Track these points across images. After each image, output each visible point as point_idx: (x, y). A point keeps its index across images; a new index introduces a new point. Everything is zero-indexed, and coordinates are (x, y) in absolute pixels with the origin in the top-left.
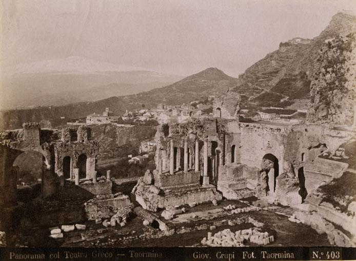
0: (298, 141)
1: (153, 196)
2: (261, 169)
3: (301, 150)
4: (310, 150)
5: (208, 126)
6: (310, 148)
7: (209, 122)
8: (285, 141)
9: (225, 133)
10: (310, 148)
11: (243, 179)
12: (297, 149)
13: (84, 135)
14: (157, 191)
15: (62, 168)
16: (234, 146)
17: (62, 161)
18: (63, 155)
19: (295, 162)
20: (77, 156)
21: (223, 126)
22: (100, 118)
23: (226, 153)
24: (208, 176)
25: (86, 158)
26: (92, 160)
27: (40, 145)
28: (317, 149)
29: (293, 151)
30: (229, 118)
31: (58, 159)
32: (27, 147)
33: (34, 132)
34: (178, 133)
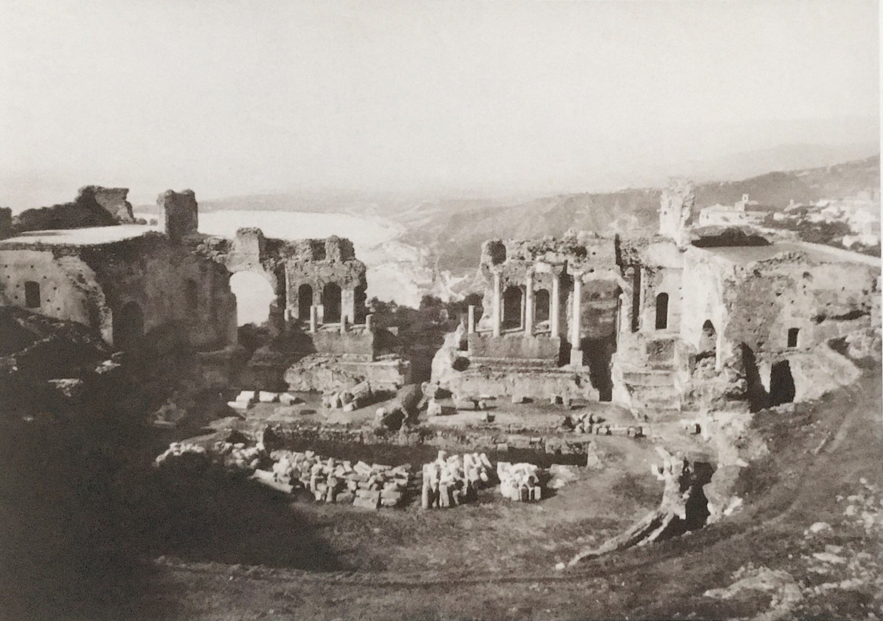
0: (778, 299)
2: (699, 352)
3: (787, 320)
4: (824, 324)
6: (820, 319)
7: (597, 241)
8: (733, 296)
9: (637, 266)
10: (820, 319)
11: (667, 368)
13: (334, 251)
15: (297, 302)
17: (297, 292)
19: (763, 347)
20: (322, 285)
21: (634, 251)
23: (641, 308)
25: (340, 290)
26: (348, 295)
28: (847, 323)
29: (759, 321)
31: (291, 287)
34: (522, 258)
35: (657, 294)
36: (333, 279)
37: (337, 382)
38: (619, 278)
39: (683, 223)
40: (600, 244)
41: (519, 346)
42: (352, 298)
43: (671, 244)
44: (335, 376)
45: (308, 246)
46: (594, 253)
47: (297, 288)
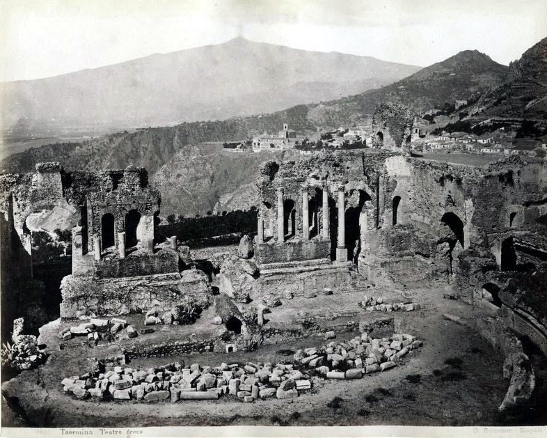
1: (245, 278)
5: (348, 164)
7: (349, 158)
12: (499, 207)
13: (134, 180)
14: (251, 271)
16: (397, 199)
18: (102, 212)
20: (124, 213)
22: (273, 142)
24: (345, 248)
25: (139, 216)
26: (148, 220)
27: (64, 196)
29: (493, 209)
30: (394, 149)
32: (43, 199)
33: (53, 176)
35: (393, 197)
36: (134, 206)
37: (156, 302)
38: (367, 186)
39: (404, 141)
40: (352, 160)
41: (300, 250)
42: (152, 223)
43: (401, 157)
44: (153, 296)
45: (108, 177)
46: (348, 168)
47: (100, 218)
